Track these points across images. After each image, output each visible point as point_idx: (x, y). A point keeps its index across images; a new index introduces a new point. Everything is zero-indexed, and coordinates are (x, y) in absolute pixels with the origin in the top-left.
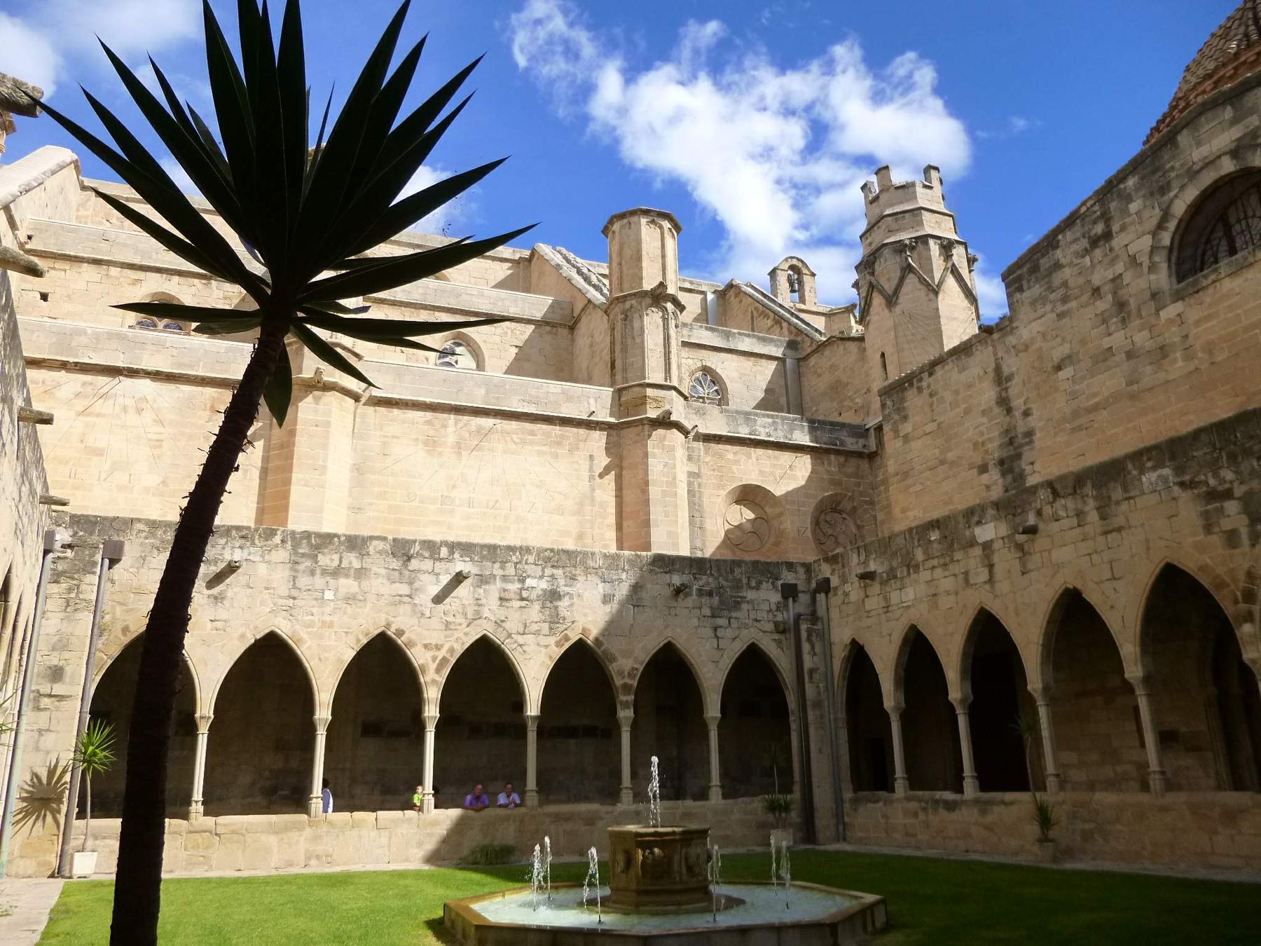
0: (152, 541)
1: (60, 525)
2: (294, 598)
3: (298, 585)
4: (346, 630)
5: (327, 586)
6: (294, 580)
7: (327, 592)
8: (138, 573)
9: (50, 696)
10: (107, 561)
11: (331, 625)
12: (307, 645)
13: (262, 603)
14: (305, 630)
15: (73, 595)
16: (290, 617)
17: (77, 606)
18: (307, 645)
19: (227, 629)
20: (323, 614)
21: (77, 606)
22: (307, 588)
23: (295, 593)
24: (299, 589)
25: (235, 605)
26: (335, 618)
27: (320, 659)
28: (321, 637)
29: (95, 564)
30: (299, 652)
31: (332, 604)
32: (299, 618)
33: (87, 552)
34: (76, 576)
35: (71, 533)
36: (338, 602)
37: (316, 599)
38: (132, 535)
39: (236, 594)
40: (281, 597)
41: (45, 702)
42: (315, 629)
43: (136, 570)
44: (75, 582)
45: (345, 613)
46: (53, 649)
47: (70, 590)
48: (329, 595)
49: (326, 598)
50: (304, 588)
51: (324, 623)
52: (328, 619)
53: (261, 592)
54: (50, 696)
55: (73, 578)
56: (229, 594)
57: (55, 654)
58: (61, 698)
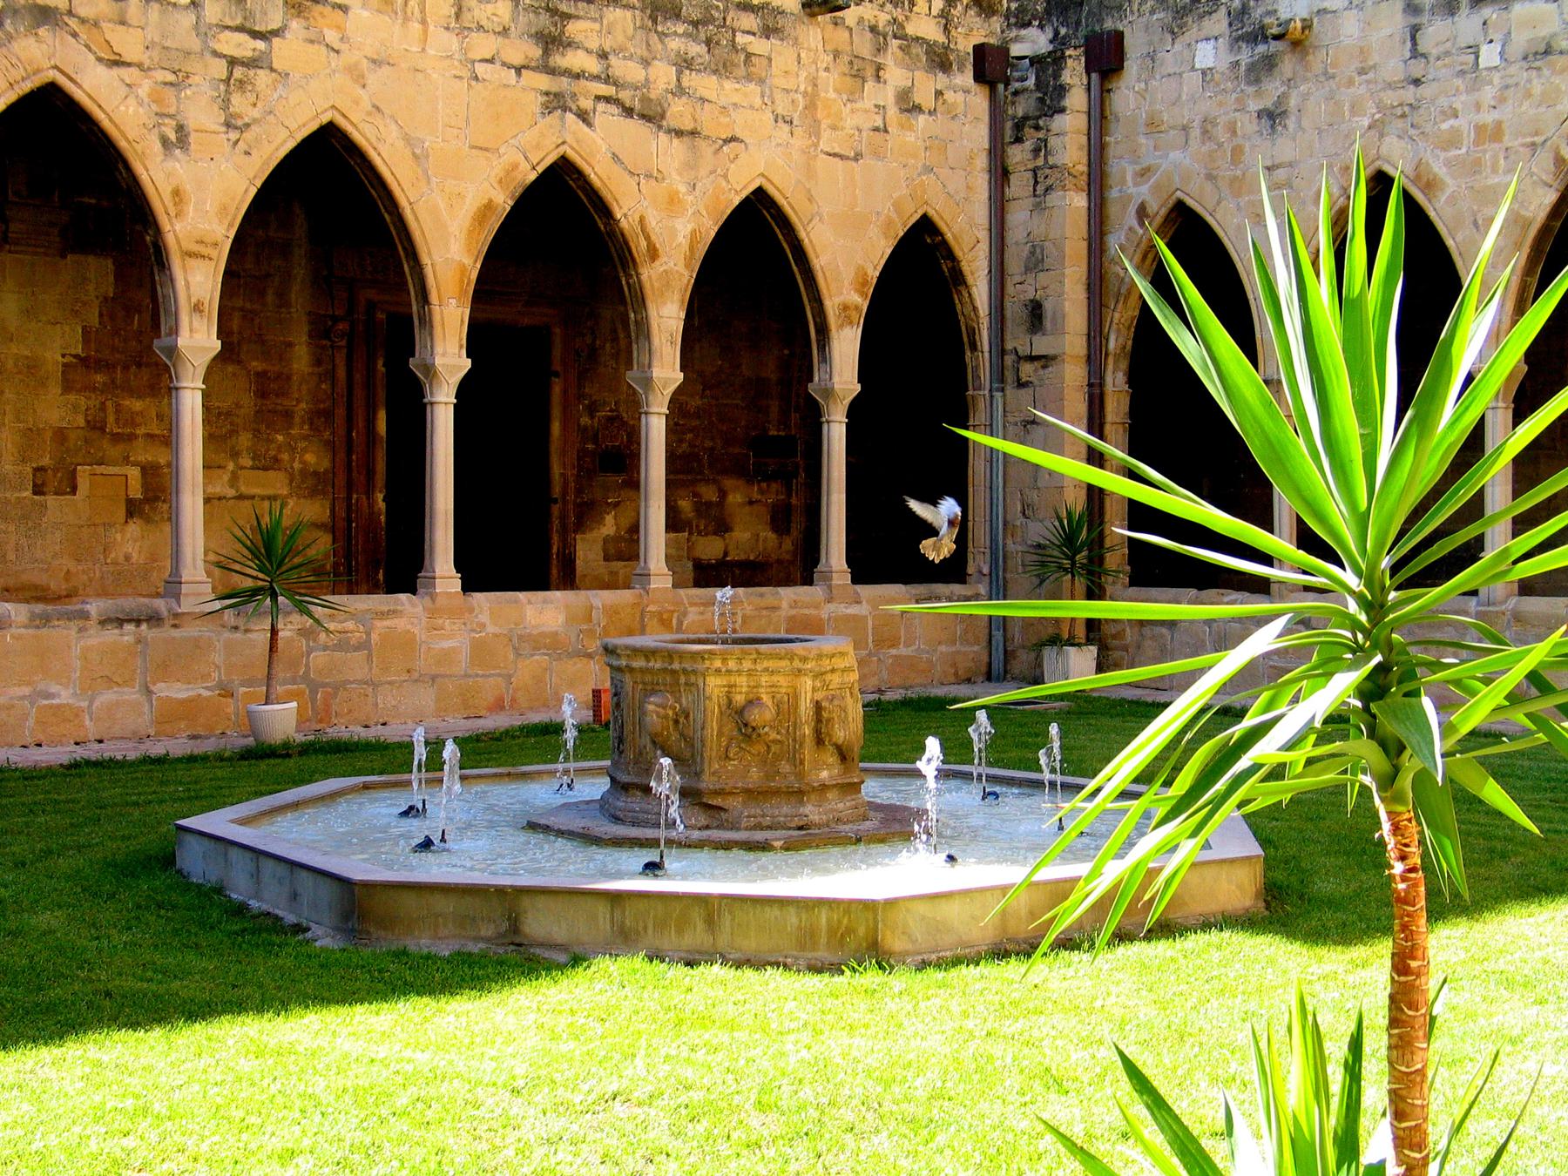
0: (1162, 15)
1: (1029, 24)
2: (1417, 82)
3: (1425, 44)
4: (1529, 140)
5: (1486, 34)
6: (1413, 38)
7: (1485, 50)
8: (1146, 90)
9: (1032, 359)
10: (1094, 76)
11: (1497, 132)
12: (1448, 192)
13: (1355, 110)
14: (1442, 155)
15: (1040, 162)
16: (1412, 132)
17: (1049, 182)
18: (1448, 192)
19: (1296, 183)
20: (1478, 107)
21: (1049, 182)
22: (1441, 49)
23: (1417, 69)
24: (1424, 56)
25: (1305, 123)
26: (1505, 114)
27: (1475, 223)
28: (1475, 167)
29: (1062, 90)
30: (1432, 214)
31: (1496, 78)
32: (1428, 128)
33: (1050, 71)
34: (1041, 123)
35: (1051, 35)
36: (1513, 70)
37: (1462, 73)
38: (1132, 11)
39: (1305, 97)
40: (1390, 86)
41: (1027, 370)
42: (1464, 150)
43: (1143, 85)
44: (1041, 135)
45: (1528, 95)
46: (1028, 270)
47: (1036, 151)
48: (1489, 56)
49: (1483, 63)
50: (1434, 52)
51: (1480, 129)
52: (1488, 118)
53: (1351, 83)
54: (1032, 359)
55: (1037, 128)
56: (1293, 102)
57: (1030, 279)
58: (1045, 360)
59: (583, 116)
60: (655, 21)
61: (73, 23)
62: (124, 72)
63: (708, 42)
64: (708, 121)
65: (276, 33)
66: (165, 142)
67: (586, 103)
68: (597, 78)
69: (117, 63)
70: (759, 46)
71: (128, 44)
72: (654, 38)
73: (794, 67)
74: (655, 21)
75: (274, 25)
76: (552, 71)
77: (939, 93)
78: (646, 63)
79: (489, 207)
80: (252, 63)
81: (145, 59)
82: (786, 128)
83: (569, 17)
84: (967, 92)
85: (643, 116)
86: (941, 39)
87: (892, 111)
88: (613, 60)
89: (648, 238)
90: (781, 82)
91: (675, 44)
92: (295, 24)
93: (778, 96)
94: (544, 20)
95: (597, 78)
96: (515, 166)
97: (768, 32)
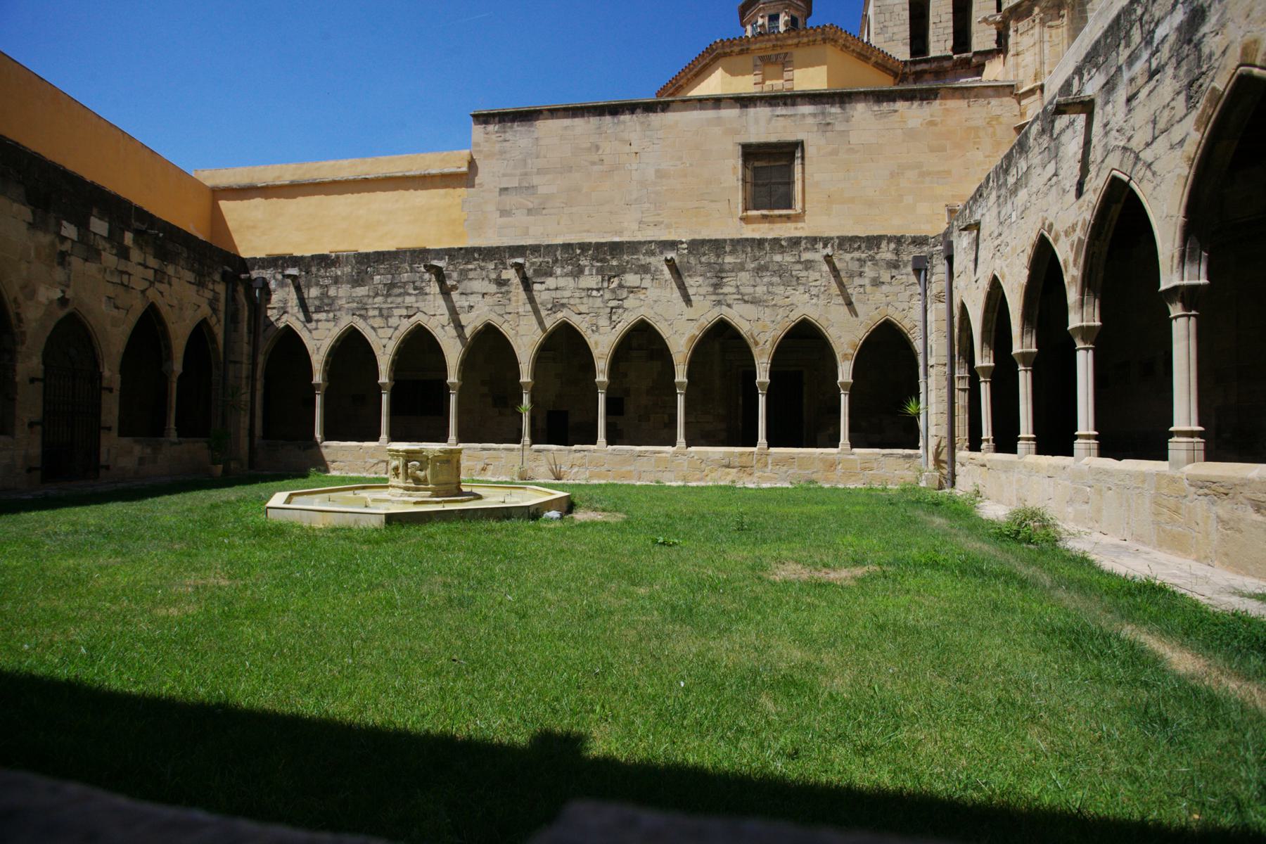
59: (729, 306)
60: (758, 273)
61: (569, 306)
62: (583, 316)
63: (780, 276)
64: (779, 300)
65: (626, 298)
66: (593, 330)
67: (729, 302)
68: (734, 294)
69: (580, 314)
70: (804, 274)
71: (583, 309)
72: (758, 279)
73: (819, 278)
74: (758, 273)
75: (624, 297)
76: (718, 294)
77: (892, 277)
78: (755, 286)
79: (694, 337)
80: (616, 308)
81: (587, 312)
82: (815, 299)
83: (722, 278)
84: (908, 274)
85: (751, 303)
86: (895, 258)
87: (869, 288)
88: (741, 287)
89: (754, 339)
90: (814, 284)
91: (765, 280)
92: (631, 295)
93: (811, 289)
94: (715, 280)
95: (734, 294)
96: (703, 323)
97: (807, 269)
